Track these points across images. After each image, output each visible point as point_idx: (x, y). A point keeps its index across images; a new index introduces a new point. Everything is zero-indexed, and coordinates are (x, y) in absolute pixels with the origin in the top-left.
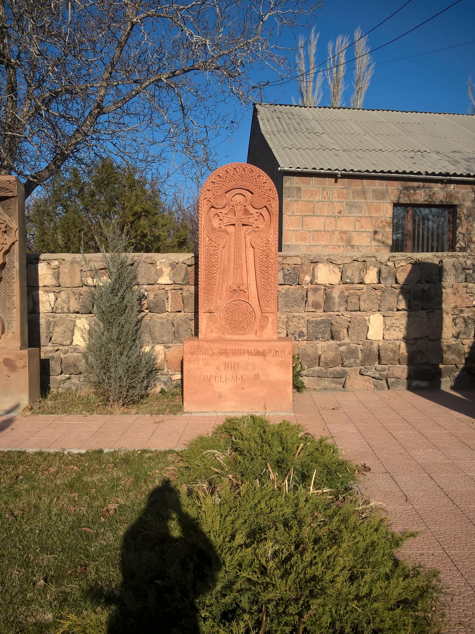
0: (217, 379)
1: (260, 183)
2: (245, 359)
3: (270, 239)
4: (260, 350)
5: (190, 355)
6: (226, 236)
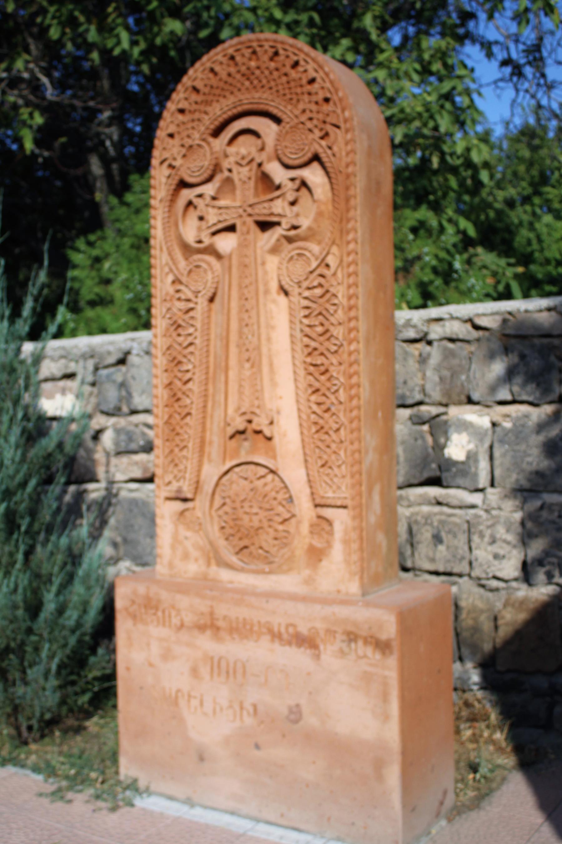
0: (195, 703)
2: (259, 652)
3: (330, 260)
4: (303, 629)
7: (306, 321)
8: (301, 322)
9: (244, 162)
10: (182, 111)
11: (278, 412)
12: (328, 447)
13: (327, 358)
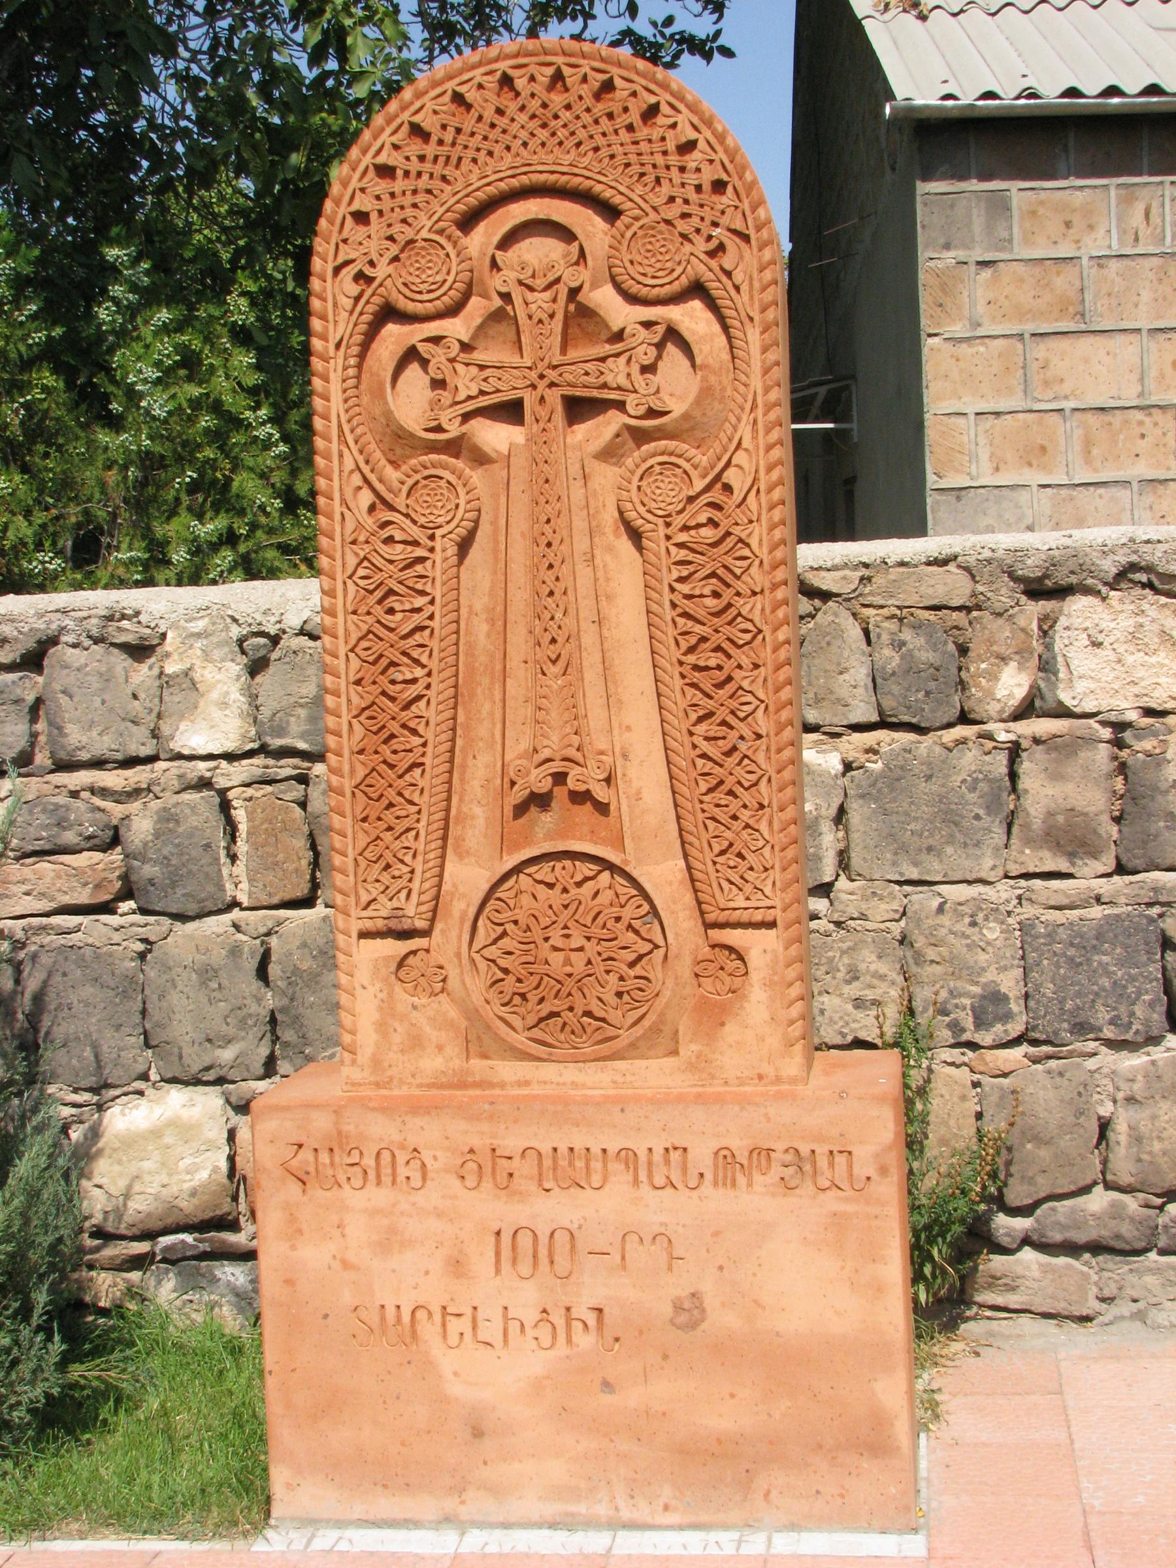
0: (454, 1325)
1: (657, 147)
3: (731, 476)
5: (295, 1187)
6: (476, 477)
7: (685, 588)
8: (672, 590)
9: (540, 283)
11: (625, 756)
12: (735, 817)
13: (729, 657)
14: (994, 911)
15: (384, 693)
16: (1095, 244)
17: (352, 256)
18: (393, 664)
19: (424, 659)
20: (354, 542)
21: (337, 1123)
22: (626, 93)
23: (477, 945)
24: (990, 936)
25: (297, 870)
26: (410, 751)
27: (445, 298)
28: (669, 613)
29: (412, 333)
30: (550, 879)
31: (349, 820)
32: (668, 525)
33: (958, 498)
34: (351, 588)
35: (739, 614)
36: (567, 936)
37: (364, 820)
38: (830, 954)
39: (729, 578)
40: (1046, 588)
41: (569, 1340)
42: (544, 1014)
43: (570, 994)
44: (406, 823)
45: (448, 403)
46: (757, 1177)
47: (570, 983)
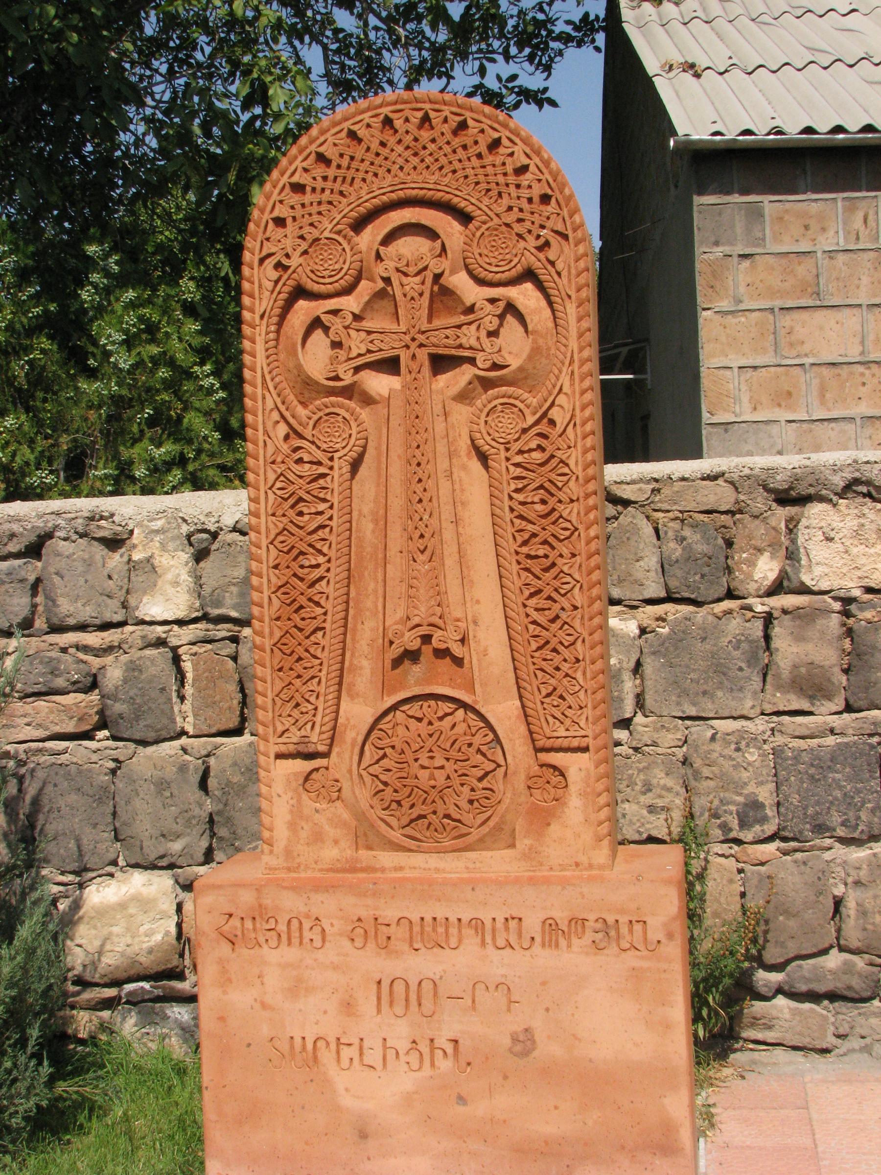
0: (346, 1052)
1: (499, 170)
3: (554, 413)
5: (226, 947)
6: (364, 414)
7: (520, 497)
8: (511, 498)
9: (412, 270)
10: (298, 188)
11: (475, 623)
12: (558, 669)
13: (553, 548)
14: (754, 740)
15: (295, 575)
16: (826, 242)
17: (273, 250)
18: (302, 553)
19: (325, 550)
20: (273, 462)
21: (258, 898)
22: (476, 131)
23: (363, 766)
24: (751, 758)
25: (230, 708)
26: (315, 618)
27: (342, 281)
28: (508, 516)
29: (317, 308)
30: (419, 715)
31: (268, 671)
32: (507, 450)
33: (726, 431)
34: (271, 496)
35: (561, 517)
36: (432, 758)
37: (280, 670)
38: (630, 772)
39: (553, 490)
40: (792, 497)
41: (433, 1064)
42: (414, 816)
43: (434, 801)
44: (311, 672)
45: (344, 359)
46: (575, 941)
47: (434, 793)
